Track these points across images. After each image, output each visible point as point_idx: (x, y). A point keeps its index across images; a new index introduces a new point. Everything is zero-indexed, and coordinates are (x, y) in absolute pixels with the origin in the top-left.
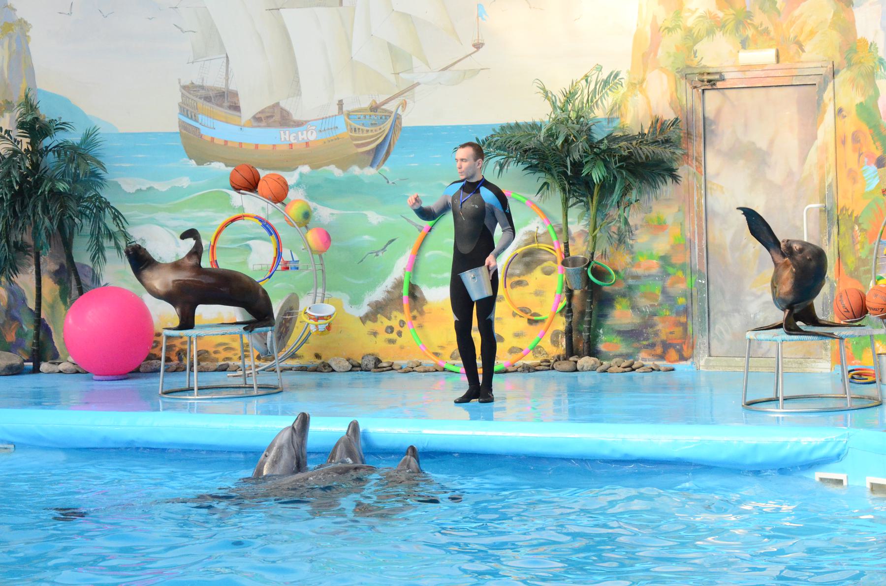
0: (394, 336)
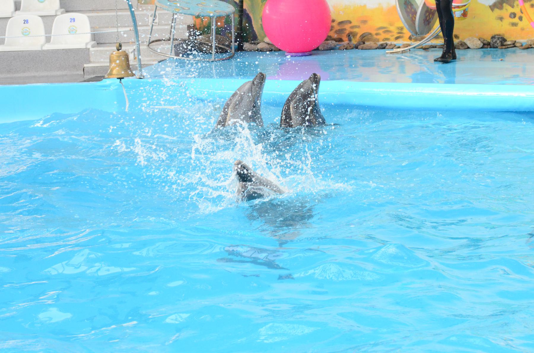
0: (516, 20)
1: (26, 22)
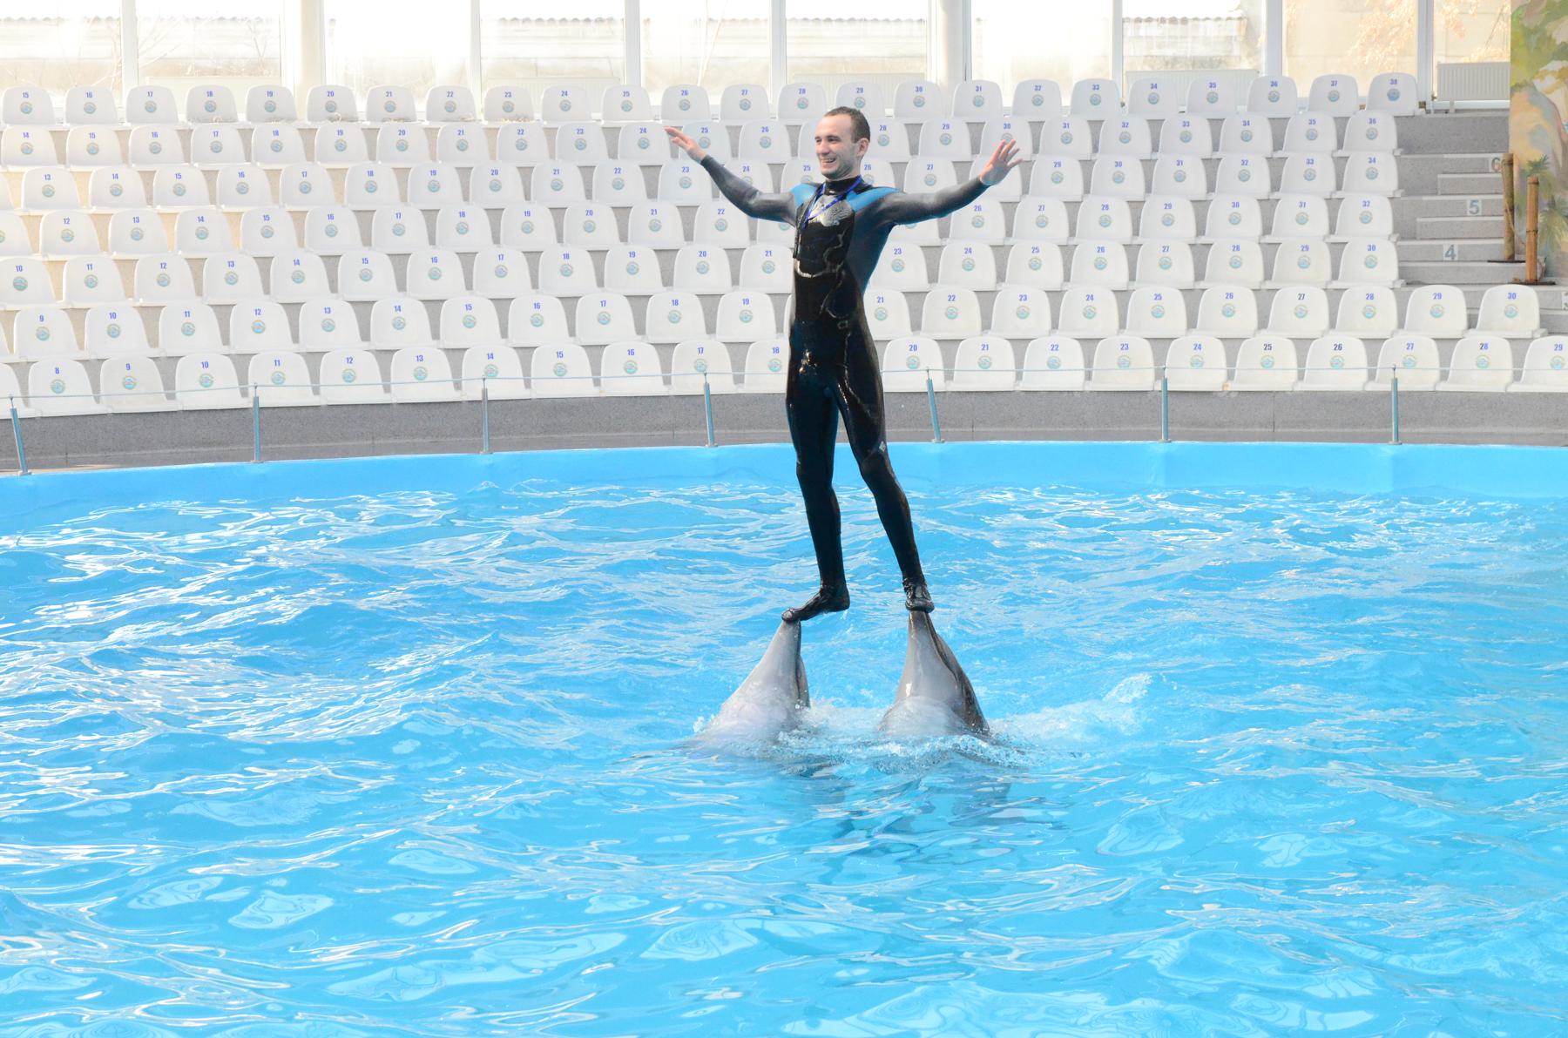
1: (1484, 346)
